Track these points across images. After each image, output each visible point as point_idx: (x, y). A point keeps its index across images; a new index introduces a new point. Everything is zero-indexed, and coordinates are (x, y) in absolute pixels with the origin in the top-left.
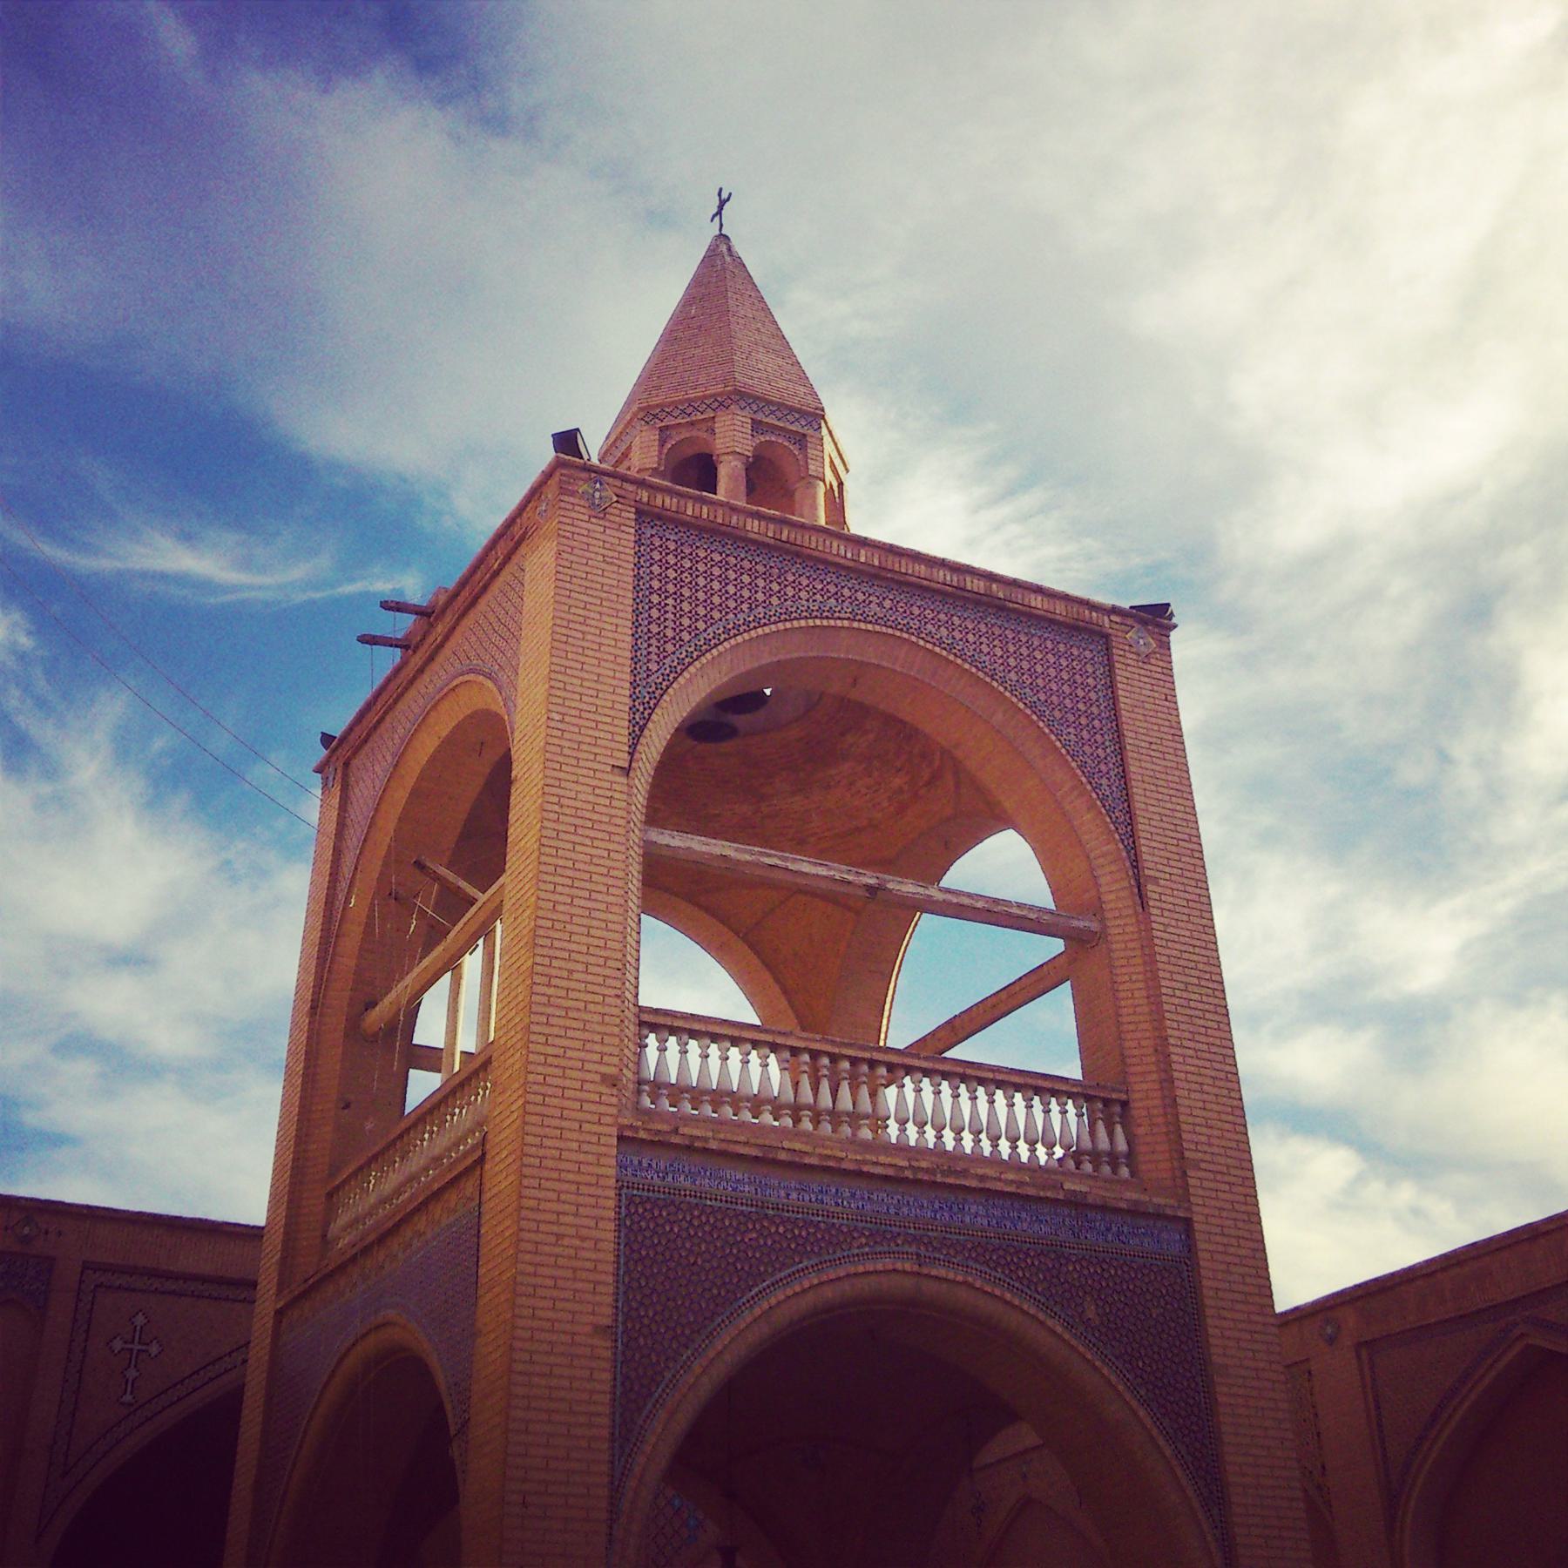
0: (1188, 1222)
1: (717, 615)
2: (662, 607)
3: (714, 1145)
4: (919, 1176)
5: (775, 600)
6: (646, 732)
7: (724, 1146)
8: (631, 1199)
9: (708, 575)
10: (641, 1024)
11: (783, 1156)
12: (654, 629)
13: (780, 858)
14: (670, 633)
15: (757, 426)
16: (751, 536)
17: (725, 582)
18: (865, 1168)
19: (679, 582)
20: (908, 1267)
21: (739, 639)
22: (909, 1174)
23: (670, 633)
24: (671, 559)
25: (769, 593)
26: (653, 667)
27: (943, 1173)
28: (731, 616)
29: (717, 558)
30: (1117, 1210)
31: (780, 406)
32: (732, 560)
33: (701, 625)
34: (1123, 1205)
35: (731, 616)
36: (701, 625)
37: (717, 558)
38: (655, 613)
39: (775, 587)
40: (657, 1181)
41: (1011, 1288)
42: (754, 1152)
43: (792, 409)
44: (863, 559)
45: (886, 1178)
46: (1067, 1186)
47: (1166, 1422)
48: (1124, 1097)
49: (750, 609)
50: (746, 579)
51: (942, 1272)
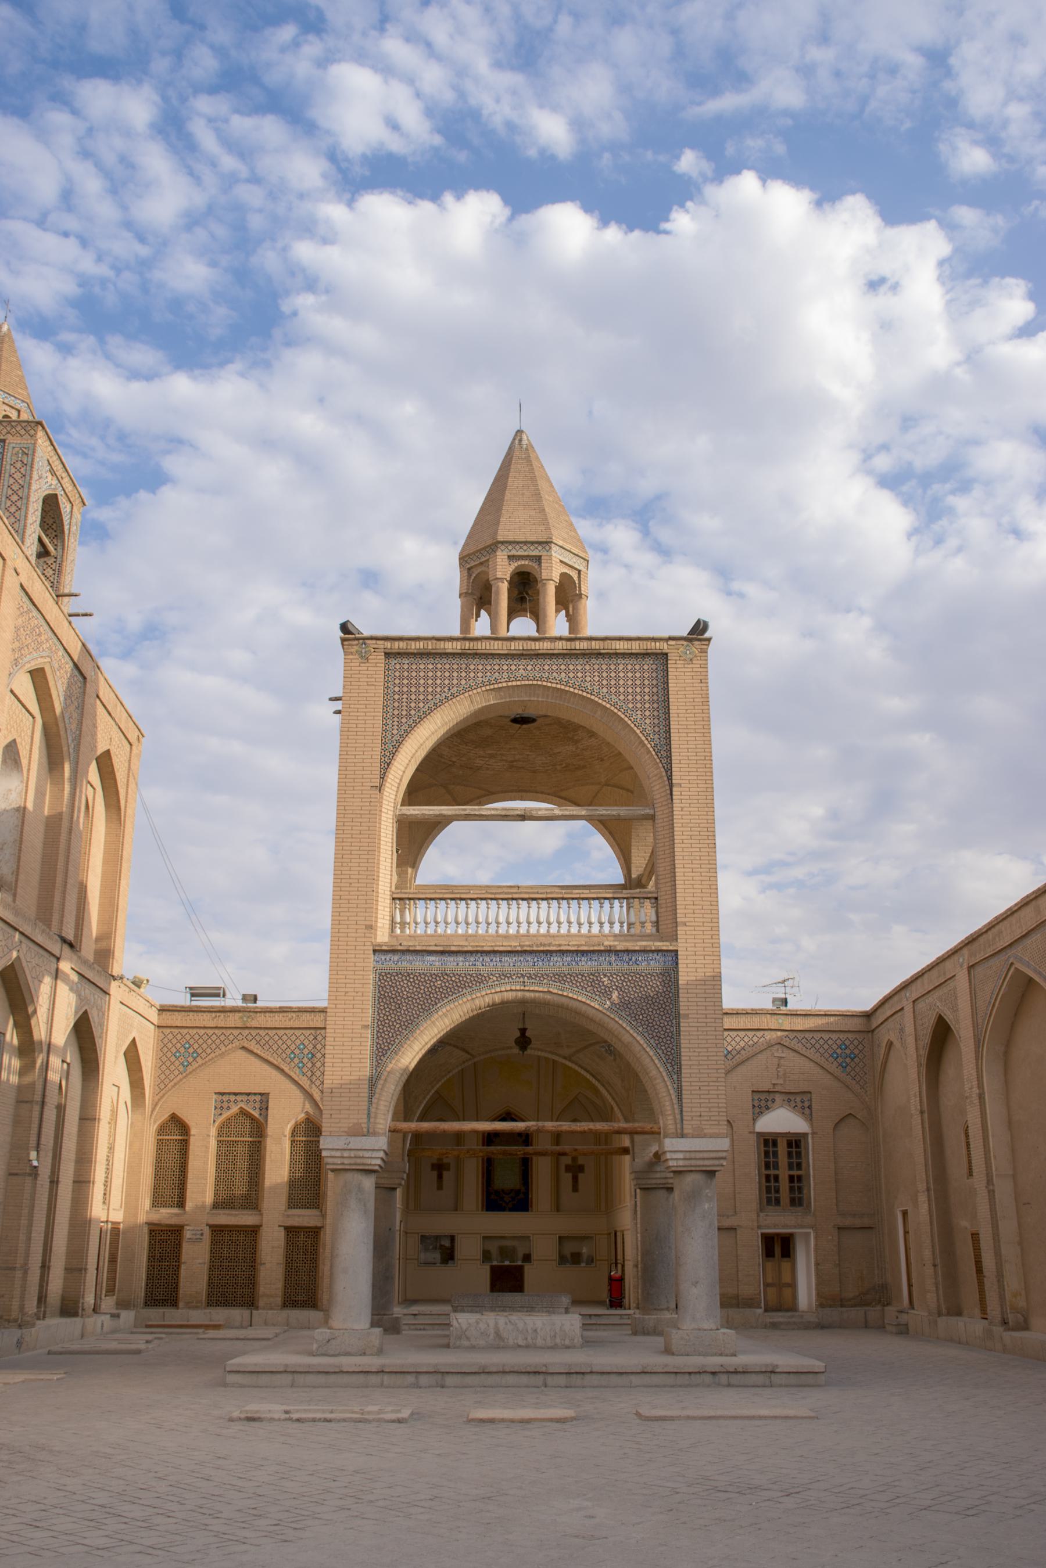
0: (677, 951)
2: (400, 701)
3: (418, 948)
4: (526, 948)
5: (463, 682)
7: (424, 948)
8: (380, 974)
9: (426, 678)
10: (394, 899)
11: (453, 949)
12: (396, 712)
15: (511, 558)
17: (435, 678)
18: (496, 949)
20: (518, 988)
22: (519, 949)
23: (404, 713)
24: (406, 674)
26: (395, 732)
27: (537, 946)
30: (635, 951)
31: (525, 543)
32: (439, 666)
34: (637, 948)
36: (421, 705)
37: (431, 666)
38: (396, 704)
39: (464, 674)
40: (393, 965)
41: (572, 991)
42: (441, 948)
43: (532, 543)
45: (509, 952)
46: (606, 943)
47: (652, 1041)
48: (655, 895)
50: (447, 674)
51: (536, 988)
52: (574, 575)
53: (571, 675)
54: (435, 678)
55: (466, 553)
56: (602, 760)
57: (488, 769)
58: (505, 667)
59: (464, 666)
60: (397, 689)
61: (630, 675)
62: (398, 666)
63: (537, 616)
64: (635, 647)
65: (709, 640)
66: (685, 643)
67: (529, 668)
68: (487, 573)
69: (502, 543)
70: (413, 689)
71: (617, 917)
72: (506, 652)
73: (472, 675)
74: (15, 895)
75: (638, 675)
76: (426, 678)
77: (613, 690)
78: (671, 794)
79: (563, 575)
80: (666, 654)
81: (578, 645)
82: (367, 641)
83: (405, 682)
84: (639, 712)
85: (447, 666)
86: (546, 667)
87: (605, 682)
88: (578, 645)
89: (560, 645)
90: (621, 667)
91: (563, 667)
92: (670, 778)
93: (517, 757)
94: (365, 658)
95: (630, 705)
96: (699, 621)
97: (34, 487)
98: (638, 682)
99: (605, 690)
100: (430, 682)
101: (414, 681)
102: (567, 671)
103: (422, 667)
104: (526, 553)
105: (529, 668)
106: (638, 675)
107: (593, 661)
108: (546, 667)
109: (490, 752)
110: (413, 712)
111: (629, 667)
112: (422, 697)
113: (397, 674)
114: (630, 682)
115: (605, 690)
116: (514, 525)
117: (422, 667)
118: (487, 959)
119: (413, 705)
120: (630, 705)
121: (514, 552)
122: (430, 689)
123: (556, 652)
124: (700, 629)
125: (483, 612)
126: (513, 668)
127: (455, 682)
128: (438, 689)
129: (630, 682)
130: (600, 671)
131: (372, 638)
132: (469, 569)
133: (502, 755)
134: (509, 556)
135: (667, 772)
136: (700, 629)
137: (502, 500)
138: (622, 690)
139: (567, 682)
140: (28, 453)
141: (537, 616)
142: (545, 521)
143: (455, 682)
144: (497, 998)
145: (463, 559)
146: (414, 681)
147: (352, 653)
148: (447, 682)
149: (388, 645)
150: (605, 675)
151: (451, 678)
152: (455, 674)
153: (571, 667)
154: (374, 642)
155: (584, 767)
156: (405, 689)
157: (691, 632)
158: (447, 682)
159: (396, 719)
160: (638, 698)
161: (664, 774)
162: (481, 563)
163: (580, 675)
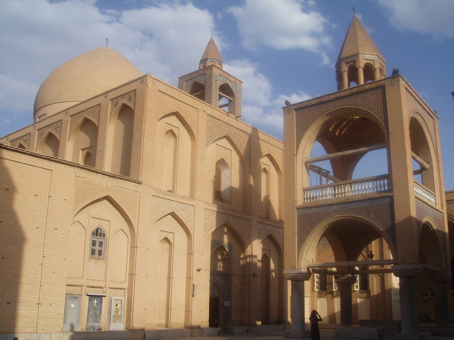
52: (372, 63)
53: (353, 101)
69: (343, 59)
71: (382, 184)
74: (230, 203)
81: (354, 90)
88: (354, 90)
92: (388, 131)
97: (213, 84)
107: (360, 94)
108: (345, 101)
111: (372, 93)
118: (331, 207)
121: (347, 61)
140: (211, 75)
144: (334, 220)
149: (295, 106)
157: (393, 75)
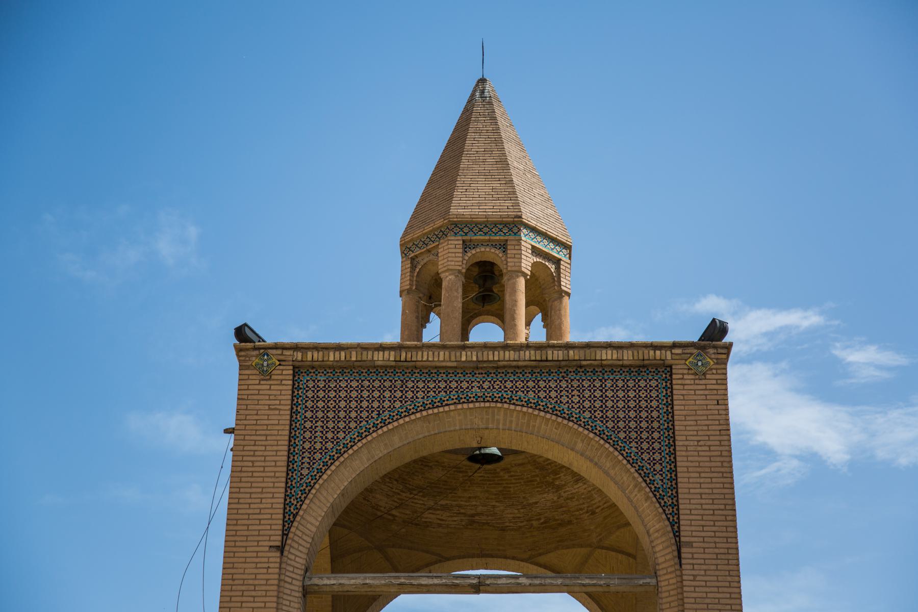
1: (353, 425)
6: (298, 518)
9: (348, 399)
12: (307, 445)
13: (405, 577)
14: (318, 446)
16: (378, 363)
19: (326, 409)
21: (369, 438)
25: (393, 400)
26: (305, 472)
28: (364, 423)
29: (354, 384)
32: (366, 383)
33: (341, 435)
35: (364, 423)
37: (354, 384)
44: (464, 359)
49: (379, 414)
54: (360, 399)
55: (408, 238)
56: (593, 513)
57: (440, 525)
58: (454, 385)
59: (399, 383)
60: (309, 414)
61: (621, 394)
62: (311, 384)
63: (502, 317)
64: (628, 356)
65: (729, 347)
66: (695, 351)
67: (486, 385)
68: (435, 264)
70: (331, 415)
72: (455, 364)
73: (410, 395)
75: (632, 394)
76: (348, 399)
77: (598, 414)
78: (680, 557)
79: (534, 265)
80: (671, 367)
82: (270, 351)
83: (321, 404)
84: (633, 444)
85: (377, 384)
86: (509, 385)
87: (587, 404)
89: (527, 355)
90: (609, 384)
91: (531, 384)
92: (677, 534)
93: (480, 509)
94: (266, 374)
95: (622, 435)
96: (714, 320)
98: (632, 404)
99: (587, 415)
100: (354, 404)
101: (332, 404)
102: (537, 389)
103: (343, 384)
104: (487, 238)
105: (486, 385)
106: (632, 394)
109: (443, 502)
110: (329, 445)
111: (620, 383)
112: (342, 425)
113: (310, 394)
114: (621, 404)
115: (587, 415)
116: (472, 200)
117: (343, 384)
119: (330, 435)
120: (622, 435)
122: (353, 415)
123: (520, 363)
124: (716, 332)
125: (433, 316)
126: (465, 385)
127: (387, 404)
128: (365, 414)
129: (621, 404)
130: (581, 389)
131: (276, 347)
132: (412, 259)
133: (460, 506)
134: (464, 241)
135: (672, 526)
136: (716, 332)
137: (457, 168)
138: (610, 414)
139: (537, 404)
141: (502, 317)
142: (512, 194)
143: (387, 404)
145: (406, 247)
146: (332, 404)
147: (248, 368)
148: (376, 404)
150: (587, 394)
151: (381, 399)
152: (387, 394)
153: (542, 384)
154: (279, 352)
155: (570, 522)
156: (320, 414)
158: (376, 404)
159: (306, 454)
160: (633, 425)
161: (669, 528)
162: (429, 251)
163: (553, 394)
